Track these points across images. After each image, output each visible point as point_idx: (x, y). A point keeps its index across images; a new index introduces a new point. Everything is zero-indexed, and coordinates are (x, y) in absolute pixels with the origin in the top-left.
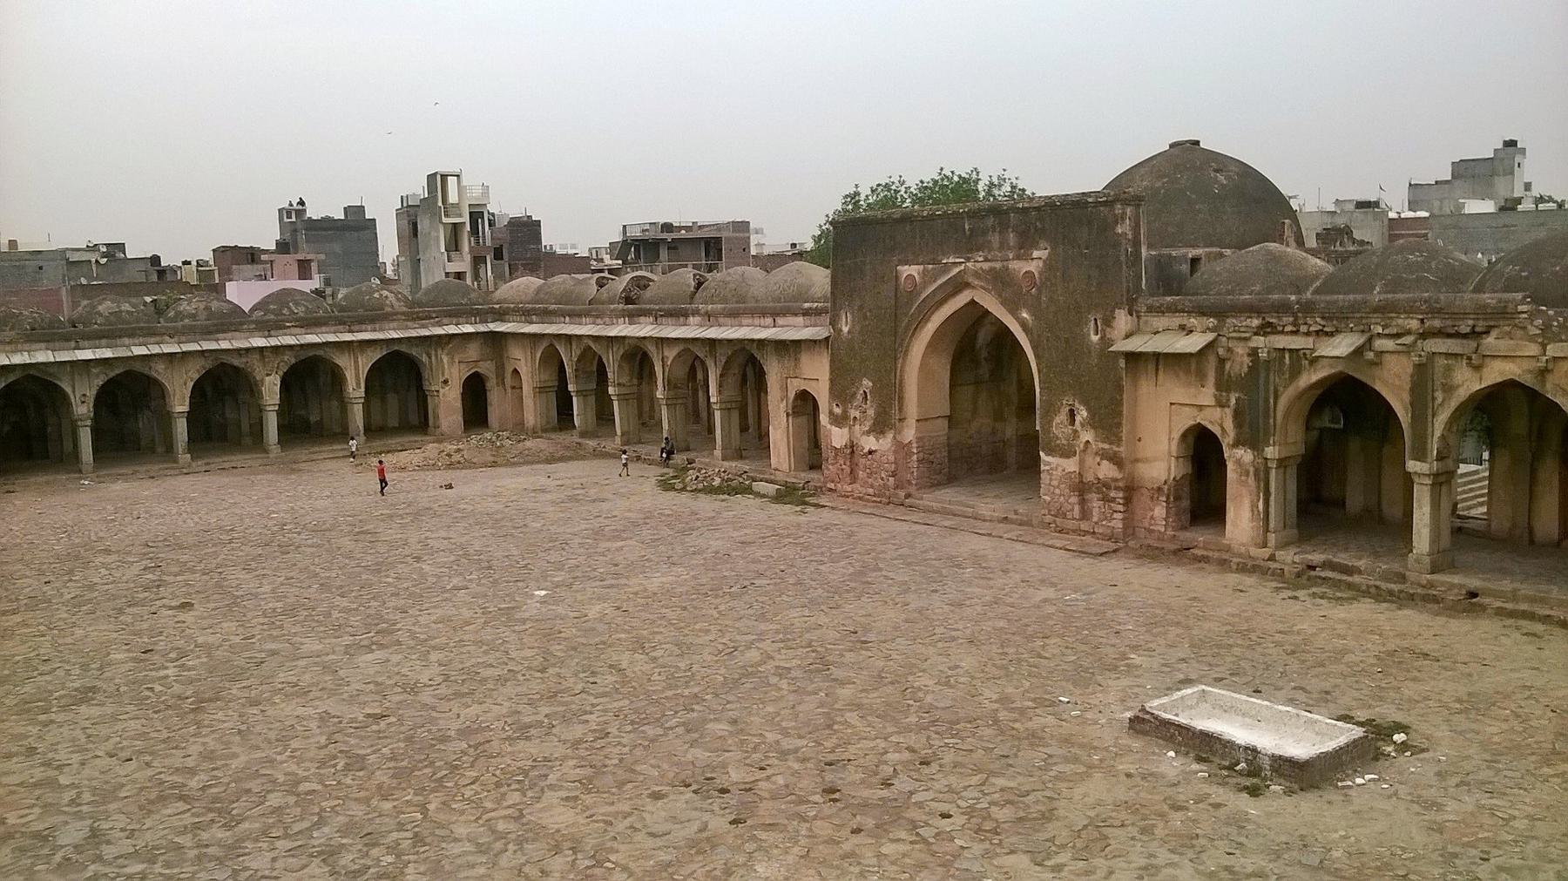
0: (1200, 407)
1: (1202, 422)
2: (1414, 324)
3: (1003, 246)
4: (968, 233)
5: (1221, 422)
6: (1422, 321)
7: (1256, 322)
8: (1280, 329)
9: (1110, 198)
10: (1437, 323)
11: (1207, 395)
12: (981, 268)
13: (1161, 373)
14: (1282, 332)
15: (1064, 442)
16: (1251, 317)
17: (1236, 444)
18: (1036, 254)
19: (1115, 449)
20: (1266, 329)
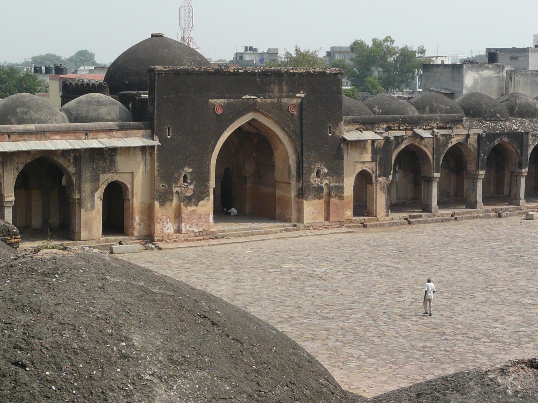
0: (364, 163)
1: (365, 169)
2: (435, 125)
3: (281, 91)
4: (259, 83)
5: (370, 167)
6: (437, 124)
7: (385, 126)
8: (393, 128)
9: (337, 72)
10: (442, 125)
11: (368, 157)
12: (266, 103)
13: (349, 149)
14: (393, 130)
15: (316, 186)
16: (383, 124)
17: (379, 176)
18: (298, 95)
19: (341, 184)
20: (389, 129)
